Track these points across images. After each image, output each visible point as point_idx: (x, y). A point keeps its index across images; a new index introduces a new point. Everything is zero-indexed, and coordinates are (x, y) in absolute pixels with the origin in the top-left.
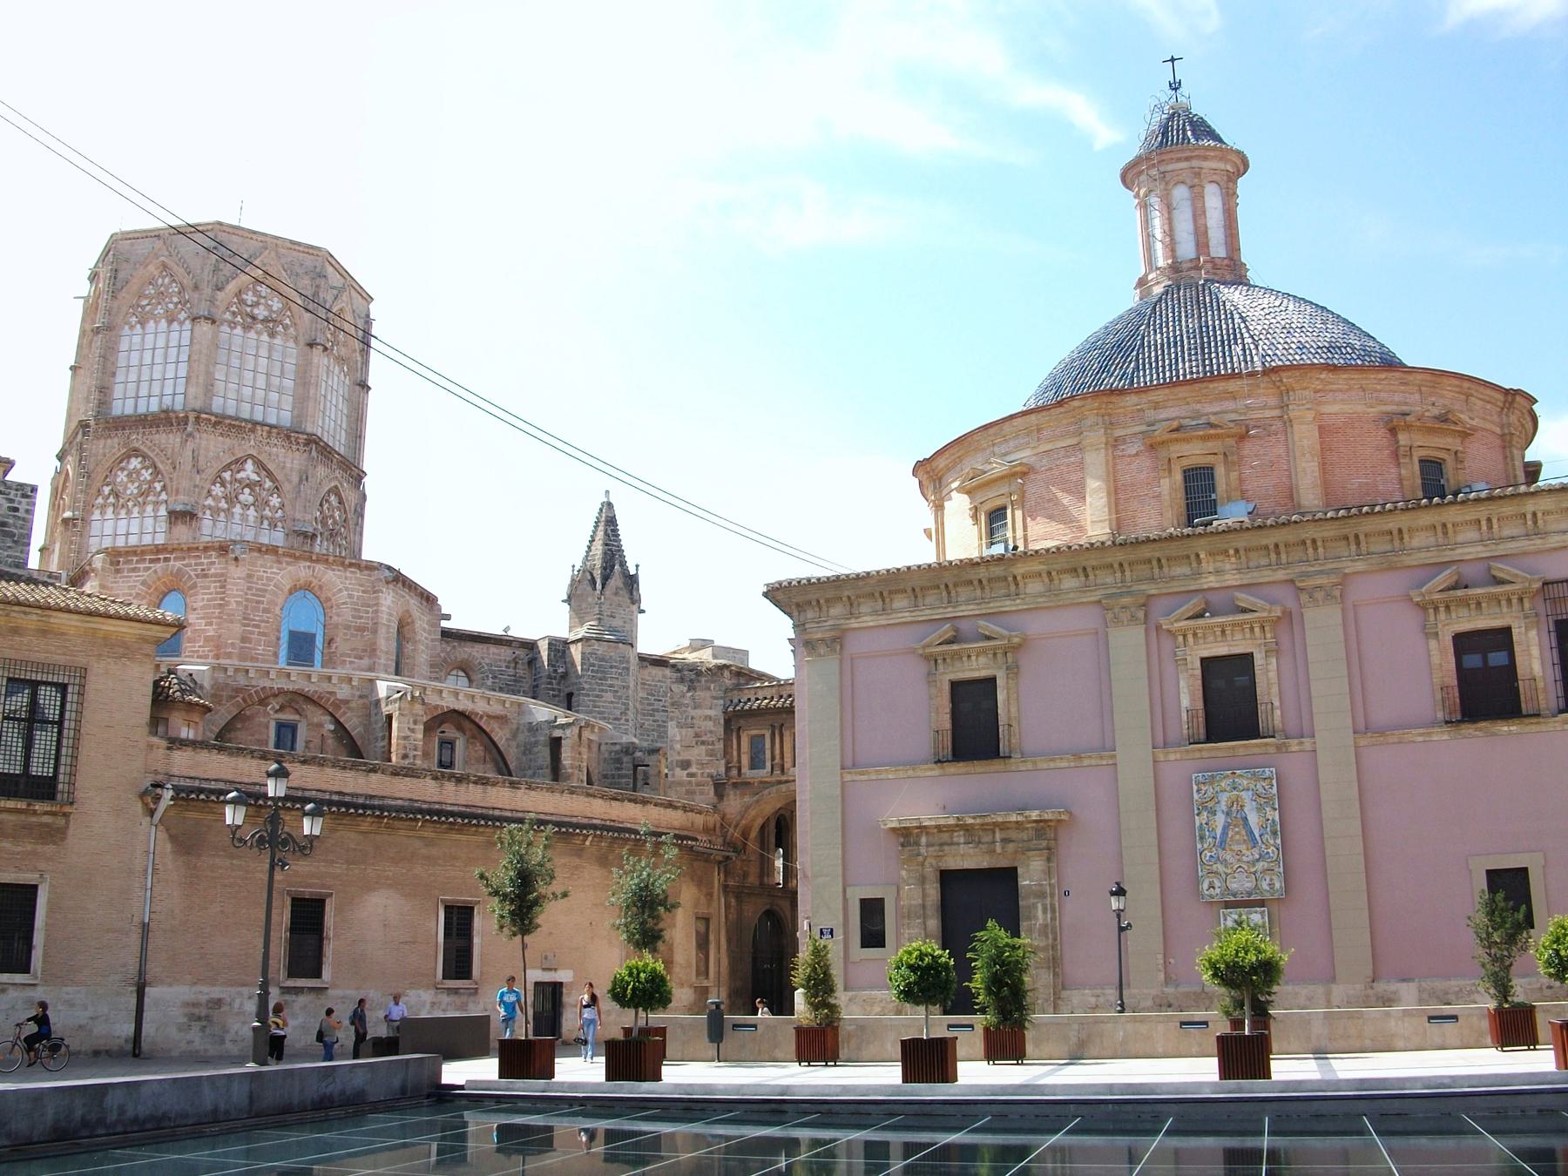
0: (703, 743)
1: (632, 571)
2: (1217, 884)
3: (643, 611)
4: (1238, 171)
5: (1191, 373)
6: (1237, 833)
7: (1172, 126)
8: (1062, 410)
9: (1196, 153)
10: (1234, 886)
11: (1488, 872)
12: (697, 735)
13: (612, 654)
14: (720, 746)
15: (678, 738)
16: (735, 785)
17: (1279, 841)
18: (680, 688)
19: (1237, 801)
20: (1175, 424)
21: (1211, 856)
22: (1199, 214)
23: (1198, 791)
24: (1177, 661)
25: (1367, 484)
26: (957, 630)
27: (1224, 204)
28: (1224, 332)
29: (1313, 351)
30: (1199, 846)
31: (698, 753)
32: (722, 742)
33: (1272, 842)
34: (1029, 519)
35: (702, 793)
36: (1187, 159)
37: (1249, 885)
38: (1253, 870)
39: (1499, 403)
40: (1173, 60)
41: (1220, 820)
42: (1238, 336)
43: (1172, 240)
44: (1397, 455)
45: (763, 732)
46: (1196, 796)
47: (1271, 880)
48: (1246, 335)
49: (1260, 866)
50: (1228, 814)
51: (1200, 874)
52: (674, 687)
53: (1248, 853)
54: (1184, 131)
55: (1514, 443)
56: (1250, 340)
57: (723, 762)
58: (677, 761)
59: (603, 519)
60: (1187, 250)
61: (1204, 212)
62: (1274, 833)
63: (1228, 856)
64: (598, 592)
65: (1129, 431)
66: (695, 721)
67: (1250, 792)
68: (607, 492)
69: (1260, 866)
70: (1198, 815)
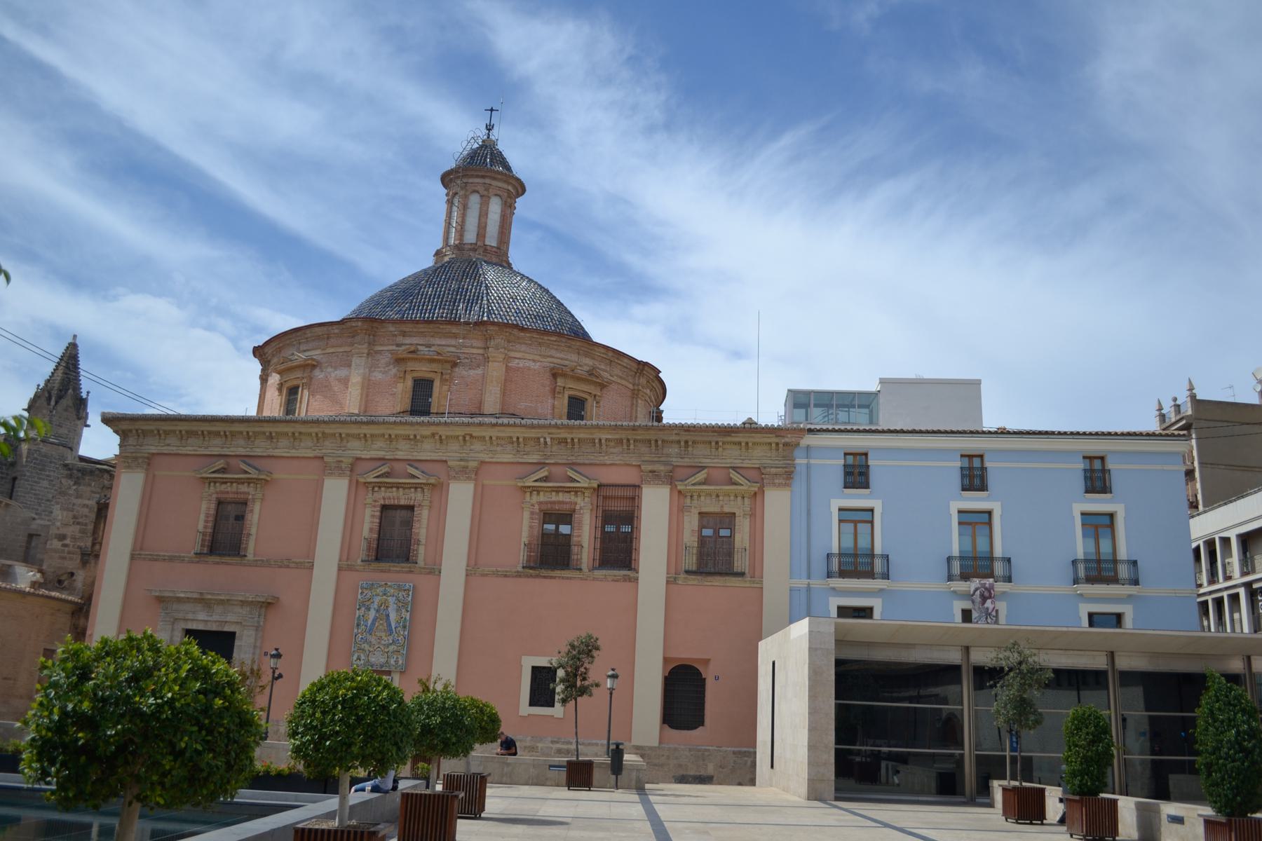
1: (84, 395)
2: (363, 657)
3: (88, 426)
4: (518, 191)
5: (442, 317)
6: (382, 624)
7: (479, 153)
8: (344, 326)
9: (488, 174)
10: (373, 660)
11: (533, 667)
12: (75, 517)
13: (54, 453)
14: (91, 527)
15: (60, 517)
17: (406, 633)
18: (67, 482)
19: (385, 603)
20: (413, 348)
21: (362, 638)
22: (483, 214)
23: (361, 593)
24: (365, 504)
25: (531, 406)
26: (228, 464)
27: (502, 211)
28: (472, 294)
29: (525, 316)
30: (356, 631)
31: (72, 530)
32: (93, 524)
33: (402, 633)
34: (311, 397)
35: (71, 559)
36: (483, 177)
37: (383, 660)
38: (386, 650)
39: (633, 369)
40: (492, 110)
41: (372, 614)
42: (480, 298)
43: (462, 228)
44: (555, 392)
46: (359, 597)
47: (397, 658)
48: (485, 299)
49: (392, 648)
50: (378, 611)
51: (353, 649)
52: (64, 481)
53: (386, 639)
54: (486, 158)
55: (640, 396)
56: (486, 302)
57: (91, 539)
58: (56, 534)
59: (68, 355)
60: (470, 237)
61: (487, 214)
62: (404, 627)
63: (373, 640)
64: (52, 407)
65: (385, 348)
66: (75, 507)
67: (395, 598)
68: (75, 336)
69: (392, 648)
70: (358, 609)
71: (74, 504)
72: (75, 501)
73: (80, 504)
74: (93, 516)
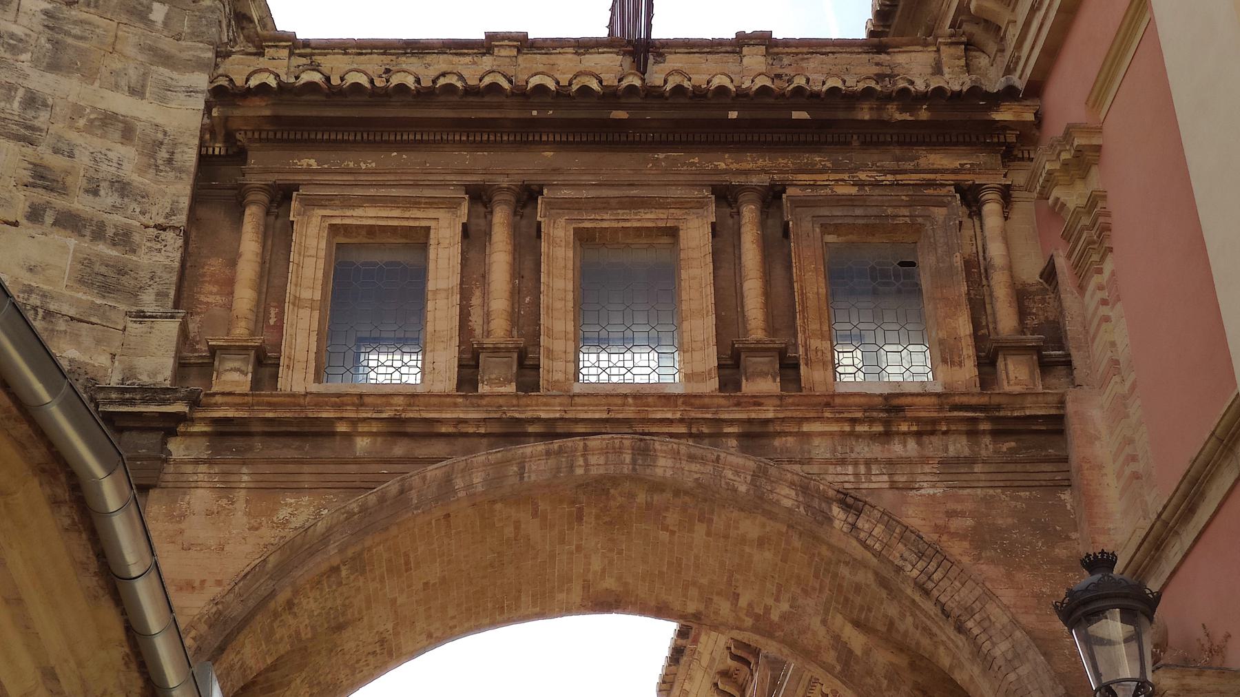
0: (70, 222)
12: (42, 177)
32: (173, 241)
45: (417, 217)
57: (171, 328)
71: (32, 101)
72: (40, 82)
73: (78, 111)
74: (179, 191)
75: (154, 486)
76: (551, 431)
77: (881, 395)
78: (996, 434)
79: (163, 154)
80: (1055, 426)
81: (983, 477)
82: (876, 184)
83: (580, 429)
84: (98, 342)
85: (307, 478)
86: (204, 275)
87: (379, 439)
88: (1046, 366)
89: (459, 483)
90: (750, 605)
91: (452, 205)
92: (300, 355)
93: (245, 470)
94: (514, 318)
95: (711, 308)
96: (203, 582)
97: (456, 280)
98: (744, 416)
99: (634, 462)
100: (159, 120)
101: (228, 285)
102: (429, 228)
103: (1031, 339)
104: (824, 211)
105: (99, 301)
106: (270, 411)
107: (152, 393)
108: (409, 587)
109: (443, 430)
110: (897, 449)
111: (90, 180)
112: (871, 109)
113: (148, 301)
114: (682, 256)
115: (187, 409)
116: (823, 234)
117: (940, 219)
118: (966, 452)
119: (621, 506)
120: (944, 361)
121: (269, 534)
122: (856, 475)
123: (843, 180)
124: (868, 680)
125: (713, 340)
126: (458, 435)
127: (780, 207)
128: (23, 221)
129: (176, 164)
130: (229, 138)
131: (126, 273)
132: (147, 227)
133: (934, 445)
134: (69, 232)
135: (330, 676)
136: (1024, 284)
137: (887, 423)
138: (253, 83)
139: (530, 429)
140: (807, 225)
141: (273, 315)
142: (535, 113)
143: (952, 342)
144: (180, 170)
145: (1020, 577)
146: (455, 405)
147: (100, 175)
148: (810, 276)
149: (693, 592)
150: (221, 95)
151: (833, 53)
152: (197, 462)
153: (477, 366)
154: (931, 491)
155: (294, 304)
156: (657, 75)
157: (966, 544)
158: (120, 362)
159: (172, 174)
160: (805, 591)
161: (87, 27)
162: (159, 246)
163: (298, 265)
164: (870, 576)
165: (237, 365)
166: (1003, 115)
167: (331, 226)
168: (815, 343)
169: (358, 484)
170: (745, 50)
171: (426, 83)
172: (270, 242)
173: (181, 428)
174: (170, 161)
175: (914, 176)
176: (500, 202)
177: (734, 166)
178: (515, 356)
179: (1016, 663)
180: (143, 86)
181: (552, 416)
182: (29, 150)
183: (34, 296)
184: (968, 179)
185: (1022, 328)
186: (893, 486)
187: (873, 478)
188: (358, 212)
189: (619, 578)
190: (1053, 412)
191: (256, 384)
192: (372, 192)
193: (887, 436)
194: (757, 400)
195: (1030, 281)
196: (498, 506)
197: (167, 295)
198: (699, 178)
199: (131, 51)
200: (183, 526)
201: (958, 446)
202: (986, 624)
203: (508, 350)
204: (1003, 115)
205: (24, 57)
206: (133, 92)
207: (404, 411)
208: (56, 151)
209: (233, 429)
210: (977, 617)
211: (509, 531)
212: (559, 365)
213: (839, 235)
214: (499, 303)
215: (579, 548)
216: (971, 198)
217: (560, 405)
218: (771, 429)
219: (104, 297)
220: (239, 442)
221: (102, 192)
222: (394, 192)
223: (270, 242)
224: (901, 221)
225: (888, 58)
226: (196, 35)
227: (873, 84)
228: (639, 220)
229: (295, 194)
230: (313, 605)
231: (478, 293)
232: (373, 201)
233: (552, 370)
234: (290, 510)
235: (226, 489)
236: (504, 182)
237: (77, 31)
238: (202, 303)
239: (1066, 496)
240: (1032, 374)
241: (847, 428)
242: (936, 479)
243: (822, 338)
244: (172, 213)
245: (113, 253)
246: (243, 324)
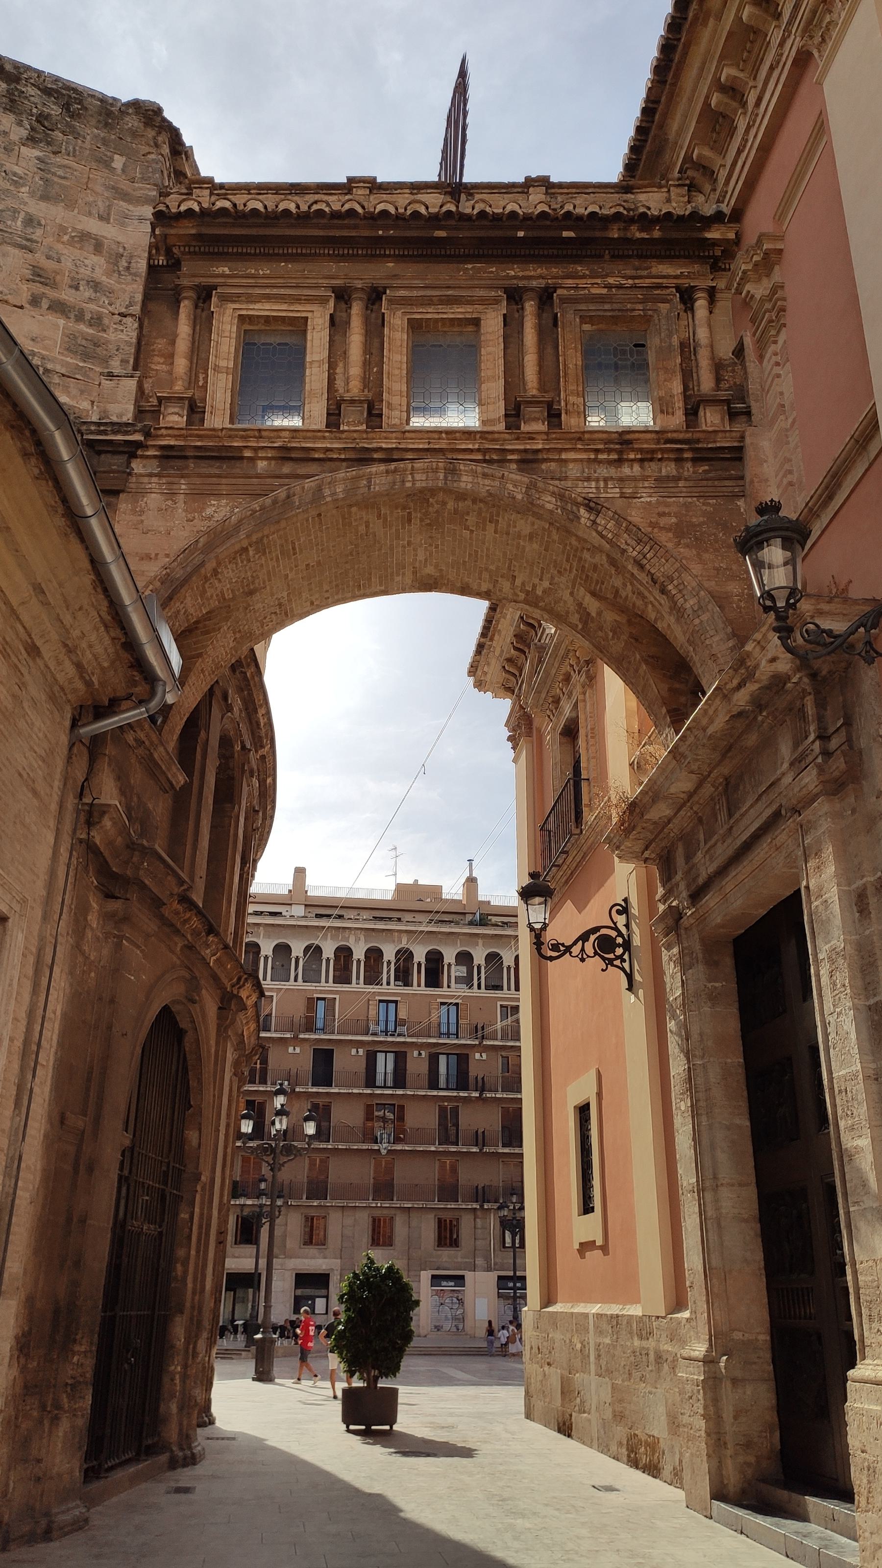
0: (59, 308)
12: (38, 275)
16: (169, 455)
32: (131, 324)
45: (298, 310)
57: (131, 384)
71: (30, 221)
73: (63, 230)
75: (123, 491)
76: (390, 457)
77: (617, 432)
78: (694, 460)
79: (124, 263)
80: (737, 454)
81: (684, 490)
82: (620, 287)
83: (410, 456)
84: (82, 392)
85: (223, 487)
86: (154, 350)
87: (273, 462)
88: (733, 415)
89: (327, 492)
90: (523, 584)
91: (323, 301)
92: (220, 406)
93: (183, 481)
94: (366, 382)
95: (502, 374)
96: (157, 555)
97: (326, 354)
98: (522, 447)
99: (446, 478)
100: (120, 239)
101: (170, 357)
102: (306, 318)
103: (723, 395)
104: (583, 307)
105: (81, 364)
106: (199, 441)
107: (119, 427)
108: (296, 566)
109: (316, 456)
110: (626, 470)
111: (73, 279)
112: (619, 229)
113: (115, 366)
114: (483, 338)
115: (142, 439)
116: (581, 323)
117: (664, 312)
118: (674, 473)
119: (437, 512)
120: (662, 412)
121: (201, 525)
122: (597, 488)
123: (597, 284)
124: (600, 633)
125: (502, 397)
126: (326, 460)
127: (552, 305)
128: (27, 306)
129: (132, 271)
130: (169, 252)
131: (99, 346)
132: (113, 314)
133: (652, 468)
134: (59, 315)
135: (247, 627)
136: (720, 359)
137: (620, 452)
138: (183, 208)
139: (375, 456)
140: (570, 316)
141: (201, 379)
142: (380, 232)
143: (668, 398)
144: (135, 275)
145: (706, 556)
146: (324, 438)
147: (80, 276)
148: (570, 352)
149: (485, 575)
150: (161, 218)
151: (594, 193)
152: (151, 475)
153: (339, 415)
154: (648, 499)
155: (215, 370)
156: (467, 207)
157: (670, 535)
158: (98, 407)
159: (129, 278)
160: (559, 572)
161: (68, 170)
162: (121, 328)
163: (217, 342)
164: (604, 558)
165: (176, 410)
166: (714, 234)
167: (240, 315)
168: (572, 399)
169: (259, 492)
170: (531, 189)
171: (304, 208)
172: (198, 327)
173: (139, 452)
174: (128, 268)
175: (647, 281)
176: (356, 299)
177: (521, 274)
178: (366, 406)
179: (700, 613)
180: (109, 214)
181: (390, 446)
182: (29, 256)
183: (36, 358)
184: (685, 282)
185: (718, 388)
186: (623, 496)
187: (609, 490)
188: (257, 306)
189: (436, 566)
190: (736, 444)
191: (189, 422)
192: (268, 291)
193: (620, 461)
194: (531, 436)
195: (725, 358)
196: (354, 509)
197: (128, 362)
198: (495, 282)
199: (99, 189)
200: (143, 518)
201: (669, 469)
202: (681, 587)
203: (361, 402)
204: (714, 234)
205: (23, 190)
206: (101, 218)
207: (289, 442)
208: (48, 257)
209: (175, 454)
210: (675, 582)
211: (362, 529)
212: (396, 413)
213: (592, 325)
214: (355, 370)
215: (409, 543)
216: (687, 297)
217: (396, 438)
218: (540, 456)
219: (85, 361)
220: (179, 463)
221: (81, 288)
222: (282, 291)
223: (198, 327)
224: (636, 313)
225: (633, 196)
226: (143, 179)
227: (621, 210)
228: (453, 313)
229: (214, 292)
230: (231, 574)
231: (341, 364)
232: (268, 298)
233: (392, 417)
234: (213, 509)
235: (172, 495)
236: (359, 284)
237: (60, 173)
238: (153, 370)
239: (741, 503)
240: (723, 419)
241: (593, 457)
242: (652, 491)
243: (578, 395)
244: (131, 304)
245: (90, 331)
246: (180, 383)
